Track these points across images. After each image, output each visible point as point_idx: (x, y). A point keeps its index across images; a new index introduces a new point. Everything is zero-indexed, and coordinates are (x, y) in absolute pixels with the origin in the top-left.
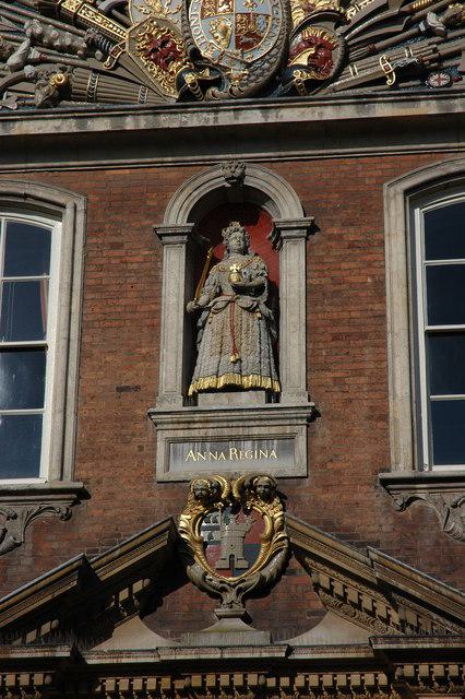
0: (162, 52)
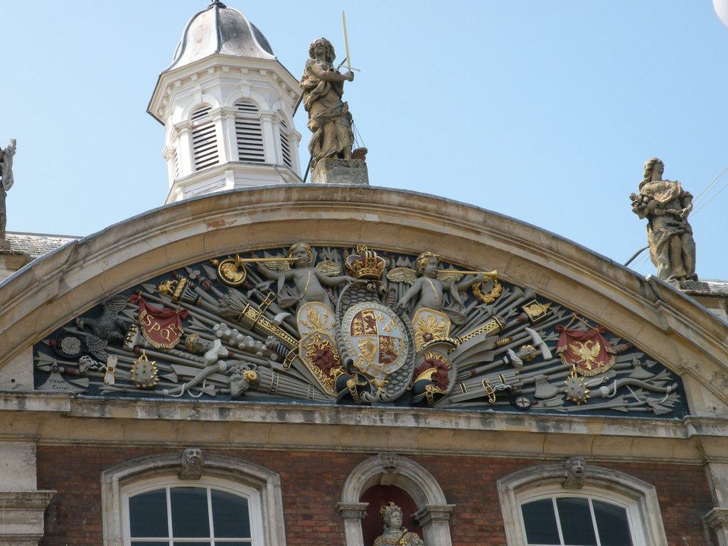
0: (325, 359)
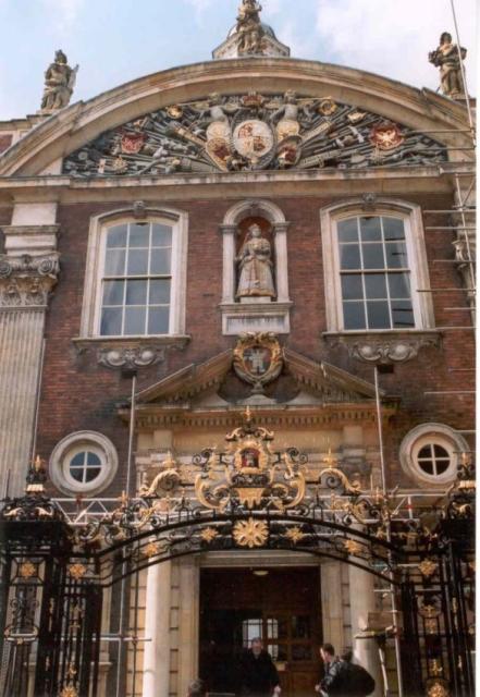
0: (221, 151)
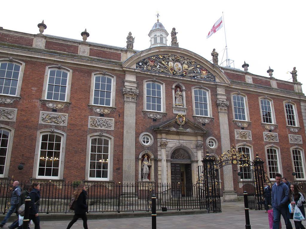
0: (172, 69)
